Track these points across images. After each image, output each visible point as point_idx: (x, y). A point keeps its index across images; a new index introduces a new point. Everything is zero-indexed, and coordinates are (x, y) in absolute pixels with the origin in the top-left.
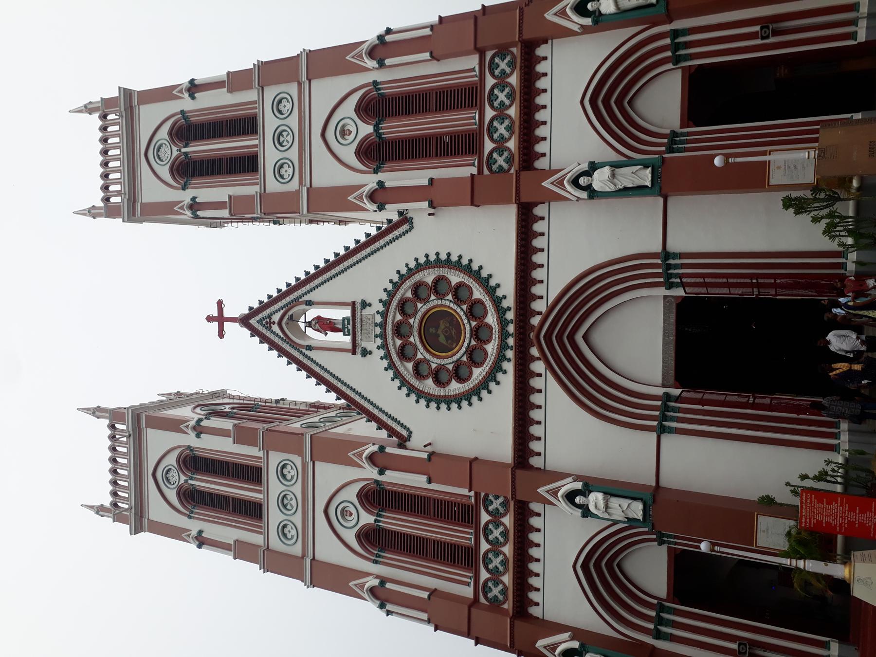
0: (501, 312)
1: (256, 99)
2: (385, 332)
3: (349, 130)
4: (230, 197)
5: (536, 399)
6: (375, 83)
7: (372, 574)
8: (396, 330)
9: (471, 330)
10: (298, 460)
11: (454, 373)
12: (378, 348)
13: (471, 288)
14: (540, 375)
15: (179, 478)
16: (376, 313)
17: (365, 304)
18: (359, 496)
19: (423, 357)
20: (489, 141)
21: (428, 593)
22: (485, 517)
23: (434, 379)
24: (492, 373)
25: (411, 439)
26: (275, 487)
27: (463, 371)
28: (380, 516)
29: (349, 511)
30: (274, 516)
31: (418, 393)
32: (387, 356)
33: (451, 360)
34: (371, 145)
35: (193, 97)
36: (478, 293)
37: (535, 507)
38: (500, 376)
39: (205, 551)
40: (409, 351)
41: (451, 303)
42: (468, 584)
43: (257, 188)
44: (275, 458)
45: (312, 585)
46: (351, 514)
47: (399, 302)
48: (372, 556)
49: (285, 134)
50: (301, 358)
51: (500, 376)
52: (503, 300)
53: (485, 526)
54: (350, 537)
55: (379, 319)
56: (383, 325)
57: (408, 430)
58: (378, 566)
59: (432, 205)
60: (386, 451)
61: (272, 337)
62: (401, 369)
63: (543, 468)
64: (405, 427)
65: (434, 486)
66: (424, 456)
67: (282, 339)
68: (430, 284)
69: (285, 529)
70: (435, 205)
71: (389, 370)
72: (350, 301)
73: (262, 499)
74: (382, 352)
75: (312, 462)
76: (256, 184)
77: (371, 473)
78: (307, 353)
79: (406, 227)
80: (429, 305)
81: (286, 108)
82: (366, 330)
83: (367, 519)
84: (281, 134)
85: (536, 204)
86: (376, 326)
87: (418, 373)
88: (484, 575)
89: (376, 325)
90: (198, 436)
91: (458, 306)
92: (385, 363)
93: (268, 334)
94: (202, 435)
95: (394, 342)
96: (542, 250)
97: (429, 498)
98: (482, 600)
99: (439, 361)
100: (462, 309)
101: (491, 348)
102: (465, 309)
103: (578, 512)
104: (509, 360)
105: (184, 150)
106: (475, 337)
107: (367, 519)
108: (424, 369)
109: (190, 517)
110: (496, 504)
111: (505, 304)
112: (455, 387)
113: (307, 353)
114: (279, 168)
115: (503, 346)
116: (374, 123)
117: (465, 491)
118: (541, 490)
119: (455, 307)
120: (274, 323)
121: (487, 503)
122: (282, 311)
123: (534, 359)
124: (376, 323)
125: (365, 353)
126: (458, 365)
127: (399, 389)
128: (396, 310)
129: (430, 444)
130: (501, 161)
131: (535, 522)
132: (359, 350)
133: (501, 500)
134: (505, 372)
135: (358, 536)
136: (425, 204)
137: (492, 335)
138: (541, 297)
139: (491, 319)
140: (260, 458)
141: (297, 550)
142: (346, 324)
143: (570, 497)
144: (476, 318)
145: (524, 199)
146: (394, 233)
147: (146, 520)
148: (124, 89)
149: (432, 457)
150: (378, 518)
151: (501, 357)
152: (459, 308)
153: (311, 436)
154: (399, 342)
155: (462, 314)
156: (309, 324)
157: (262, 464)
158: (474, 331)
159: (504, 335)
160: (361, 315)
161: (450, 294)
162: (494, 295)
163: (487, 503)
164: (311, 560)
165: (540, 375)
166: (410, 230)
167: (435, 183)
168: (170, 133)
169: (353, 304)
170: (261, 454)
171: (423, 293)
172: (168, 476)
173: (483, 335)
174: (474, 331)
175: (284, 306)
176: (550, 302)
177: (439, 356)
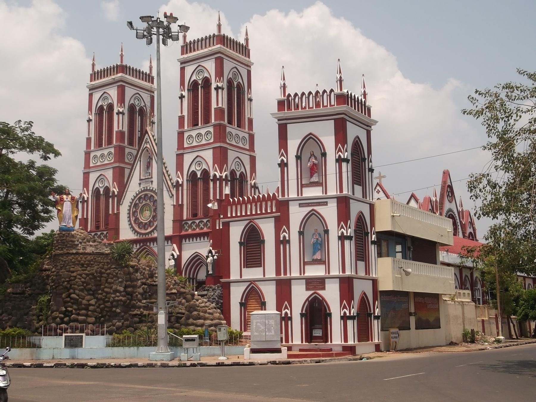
0: (150, 232)
18: (107, 186)
28: (103, 196)
30: (98, 153)
39: (87, 123)
50: (138, 158)
55: (148, 188)
57: (122, 204)
61: (143, 145)
62: (136, 199)
64: (123, 202)
79: (171, 195)
83: (102, 190)
89: (147, 187)
99: (139, 212)
104: (140, 236)
107: (102, 190)
111: (152, 233)
113: (139, 162)
114: (190, 137)
115: (143, 234)
119: (151, 216)
120: (147, 144)
132: (141, 181)
134: (137, 235)
139: (150, 230)
159: (146, 234)
169: (152, 178)
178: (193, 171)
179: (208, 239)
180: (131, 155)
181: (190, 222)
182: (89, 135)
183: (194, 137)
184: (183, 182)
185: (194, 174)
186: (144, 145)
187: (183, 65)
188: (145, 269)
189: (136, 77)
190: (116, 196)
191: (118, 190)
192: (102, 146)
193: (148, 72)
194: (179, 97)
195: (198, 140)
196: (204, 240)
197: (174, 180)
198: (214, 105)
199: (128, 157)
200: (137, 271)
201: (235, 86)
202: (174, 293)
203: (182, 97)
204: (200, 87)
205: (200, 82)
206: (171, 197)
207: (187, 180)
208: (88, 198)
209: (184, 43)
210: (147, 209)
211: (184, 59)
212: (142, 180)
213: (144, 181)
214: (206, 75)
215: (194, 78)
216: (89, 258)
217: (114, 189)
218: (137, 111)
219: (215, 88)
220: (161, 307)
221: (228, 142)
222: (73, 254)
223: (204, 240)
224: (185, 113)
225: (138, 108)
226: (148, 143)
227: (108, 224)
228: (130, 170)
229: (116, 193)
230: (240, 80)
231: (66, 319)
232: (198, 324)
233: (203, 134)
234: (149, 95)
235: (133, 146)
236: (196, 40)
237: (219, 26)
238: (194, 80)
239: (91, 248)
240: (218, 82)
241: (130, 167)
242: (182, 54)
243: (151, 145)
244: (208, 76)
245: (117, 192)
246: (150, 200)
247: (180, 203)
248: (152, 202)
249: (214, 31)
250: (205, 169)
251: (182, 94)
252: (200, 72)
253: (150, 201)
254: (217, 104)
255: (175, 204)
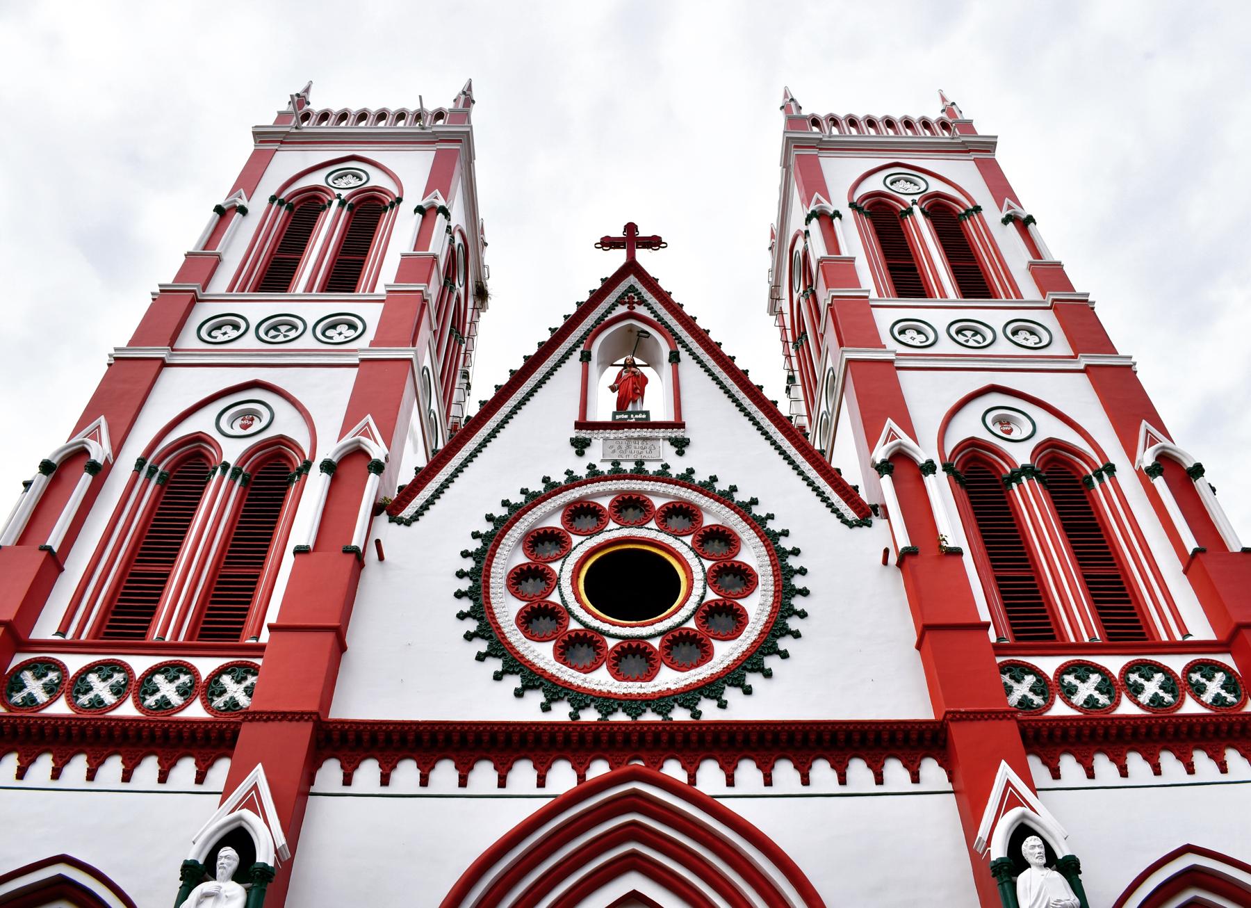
0: (688, 696)
1: (1026, 298)
2: (625, 478)
3: (1012, 430)
4: (852, 260)
5: (484, 775)
6: (1110, 469)
8: (631, 497)
9: (641, 638)
10: (364, 343)
11: (539, 605)
12: (591, 467)
13: (736, 638)
14: (541, 783)
15: (345, 187)
16: (663, 463)
17: (681, 445)
18: (282, 440)
19: (574, 545)
20: (1057, 666)
21: (56, 549)
22: (206, 666)
23: (525, 568)
24: (543, 681)
25: (394, 525)
26: (312, 312)
27: (545, 624)
29: (251, 425)
30: (257, 310)
31: (495, 535)
32: (573, 481)
33: (570, 598)
34: (992, 465)
35: (1005, 221)
36: (725, 652)
37: (220, 771)
38: (536, 698)
39: (210, 216)
40: (587, 523)
41: (698, 599)
42: (62, 631)
43: (873, 295)
44: (372, 314)
45: (113, 362)
46: (245, 427)
47: (690, 504)
48: (154, 460)
49: (979, 338)
51: (537, 698)
52: (715, 703)
53: (186, 667)
54: (202, 423)
55: (652, 468)
56: (639, 473)
57: (415, 518)
59: (905, 557)
60: (372, 475)
63: (313, 789)
65: (289, 560)
66: (357, 541)
68: (737, 559)
69: (231, 327)
70: (910, 561)
71: (543, 486)
72: (685, 418)
73: (294, 291)
74: (581, 472)
75: (358, 362)
76: (880, 294)
77: (329, 448)
78: (577, 354)
79: (851, 515)
80: (690, 557)
82: (628, 447)
83: (232, 452)
84: (976, 333)
85: (946, 763)
86: (636, 464)
87: (538, 540)
90: (419, 209)
91: (694, 613)
92: (560, 478)
94: (419, 216)
95: (604, 494)
96: (843, 781)
97: (261, 565)
98: (19, 659)
100: (687, 620)
101: (601, 680)
102: (687, 625)
103: (196, 853)
105: (916, 209)
106: (626, 645)
108: (550, 550)
109: (273, 199)
110: (234, 690)
112: (508, 608)
115: (606, 702)
116: (1037, 468)
117: (272, 617)
118: (258, 775)
119: (691, 605)
121: (240, 672)
123: (581, 769)
124: (643, 464)
125: (580, 446)
126: (558, 615)
127: (503, 501)
128: (675, 497)
129: (381, 558)
130: (1022, 689)
131: (186, 769)
132: (584, 434)
133: (244, 701)
134: (546, 708)
135: (198, 438)
136: (904, 541)
137: (635, 681)
138: (730, 782)
139: (668, 679)
140: (372, 290)
141: (189, 340)
142: (636, 416)
143: (239, 838)
144: (667, 647)
145: (958, 732)
146: (834, 493)
147: (276, 148)
148: (995, 144)
149: (352, 556)
150: (229, 471)
151: (580, 698)
152: (689, 613)
153: (410, 360)
154: (605, 503)
155: (676, 619)
156: (629, 365)
157: (360, 293)
158: (638, 645)
159: (634, 704)
160: (657, 439)
161: (717, 597)
162: (725, 682)
163: (240, 671)
164: (162, 359)
165: (541, 783)
166: (845, 522)
167: (951, 559)
168: (938, 195)
169: (681, 425)
170: (380, 289)
171: (716, 547)
172: (350, 176)
173: (632, 663)
174: (638, 645)
175: (660, 319)
176: (725, 802)
177: (578, 577)
213: (612, 434)
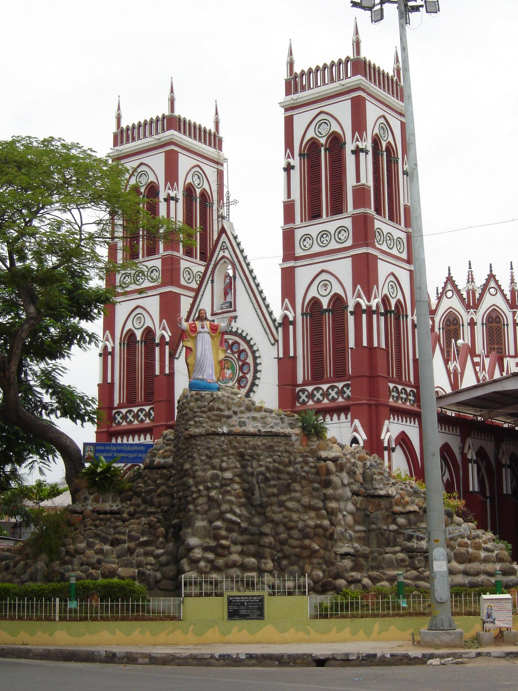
7: (114, 344)
17: (236, 317)
50: (207, 276)
57: (179, 357)
58: (119, 347)
61: (217, 252)
64: (180, 355)
67: (216, 260)
79: (273, 341)
81: (344, 236)
83: (139, 334)
88: (124, 411)
93: (218, 249)
107: (139, 334)
113: (210, 282)
119: (236, 379)
120: (224, 252)
122: (231, 259)
169: (235, 310)
178: (314, 298)
179: (346, 418)
180: (189, 273)
181: (310, 388)
182: (289, 196)
183: (315, 238)
184: (295, 318)
185: (315, 303)
186: (219, 253)
187: (290, 113)
188: (354, 464)
189: (195, 137)
190: (167, 343)
191: (170, 334)
192: (138, 258)
193: (213, 130)
194: (284, 169)
195: (322, 243)
196: (339, 419)
197: (278, 314)
198: (351, 181)
199: (185, 275)
200: (341, 468)
201: (384, 149)
202: (414, 512)
203: (288, 168)
204: (323, 149)
205: (323, 141)
206: (273, 345)
207: (303, 314)
208: (113, 348)
209: (291, 75)
210: (226, 366)
211: (292, 102)
212: (217, 314)
213: (220, 316)
214: (335, 128)
215: (311, 134)
216: (252, 441)
217: (163, 332)
218: (198, 196)
219: (353, 152)
220: (436, 539)
221: (378, 246)
222: (223, 434)
223: (339, 419)
224: (296, 195)
225: (198, 191)
226: (226, 251)
227: (153, 393)
228: (192, 299)
229: (168, 339)
230: (391, 139)
231: (221, 562)
232: (472, 571)
233: (332, 232)
234: (216, 170)
235: (192, 257)
236: (314, 68)
237: (357, 44)
238: (312, 138)
239: (256, 424)
240: (357, 140)
241: (193, 294)
242: (288, 92)
243: (232, 253)
244: (339, 131)
245: (170, 337)
246: (232, 350)
247: (292, 354)
248: (235, 353)
249: (348, 52)
250: (336, 294)
251: (289, 164)
252: (321, 124)
253: (233, 353)
254: (358, 179)
255: (281, 356)
